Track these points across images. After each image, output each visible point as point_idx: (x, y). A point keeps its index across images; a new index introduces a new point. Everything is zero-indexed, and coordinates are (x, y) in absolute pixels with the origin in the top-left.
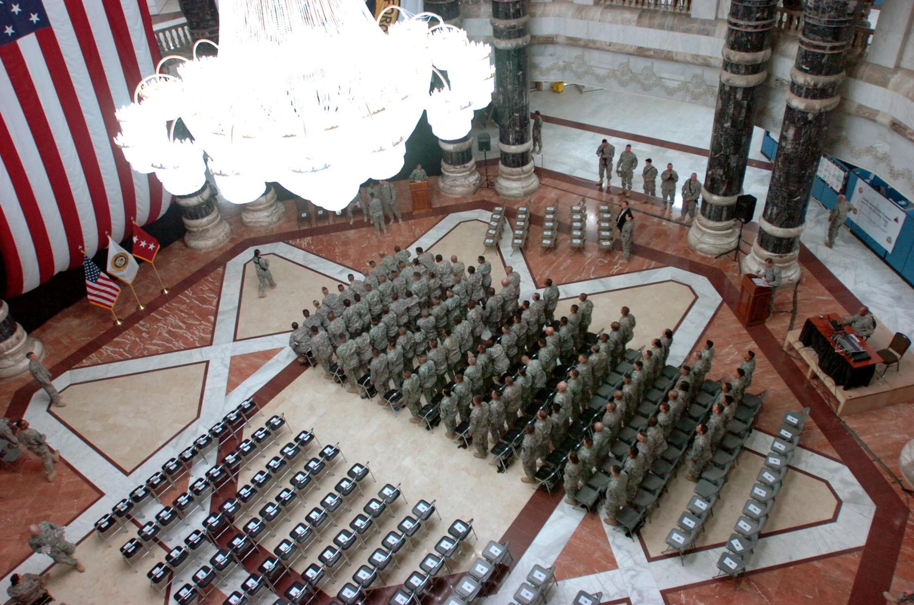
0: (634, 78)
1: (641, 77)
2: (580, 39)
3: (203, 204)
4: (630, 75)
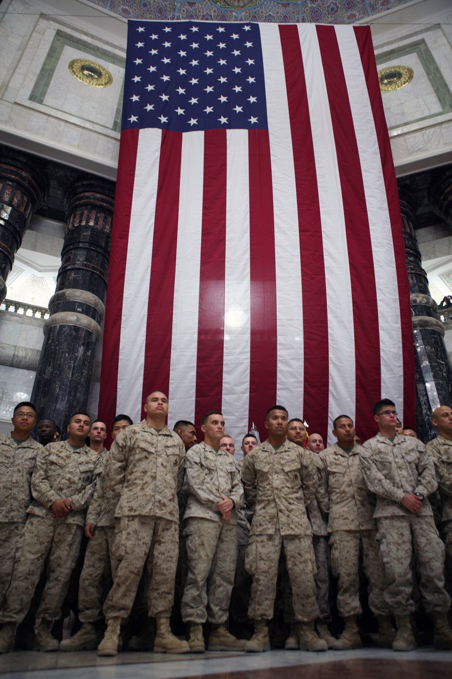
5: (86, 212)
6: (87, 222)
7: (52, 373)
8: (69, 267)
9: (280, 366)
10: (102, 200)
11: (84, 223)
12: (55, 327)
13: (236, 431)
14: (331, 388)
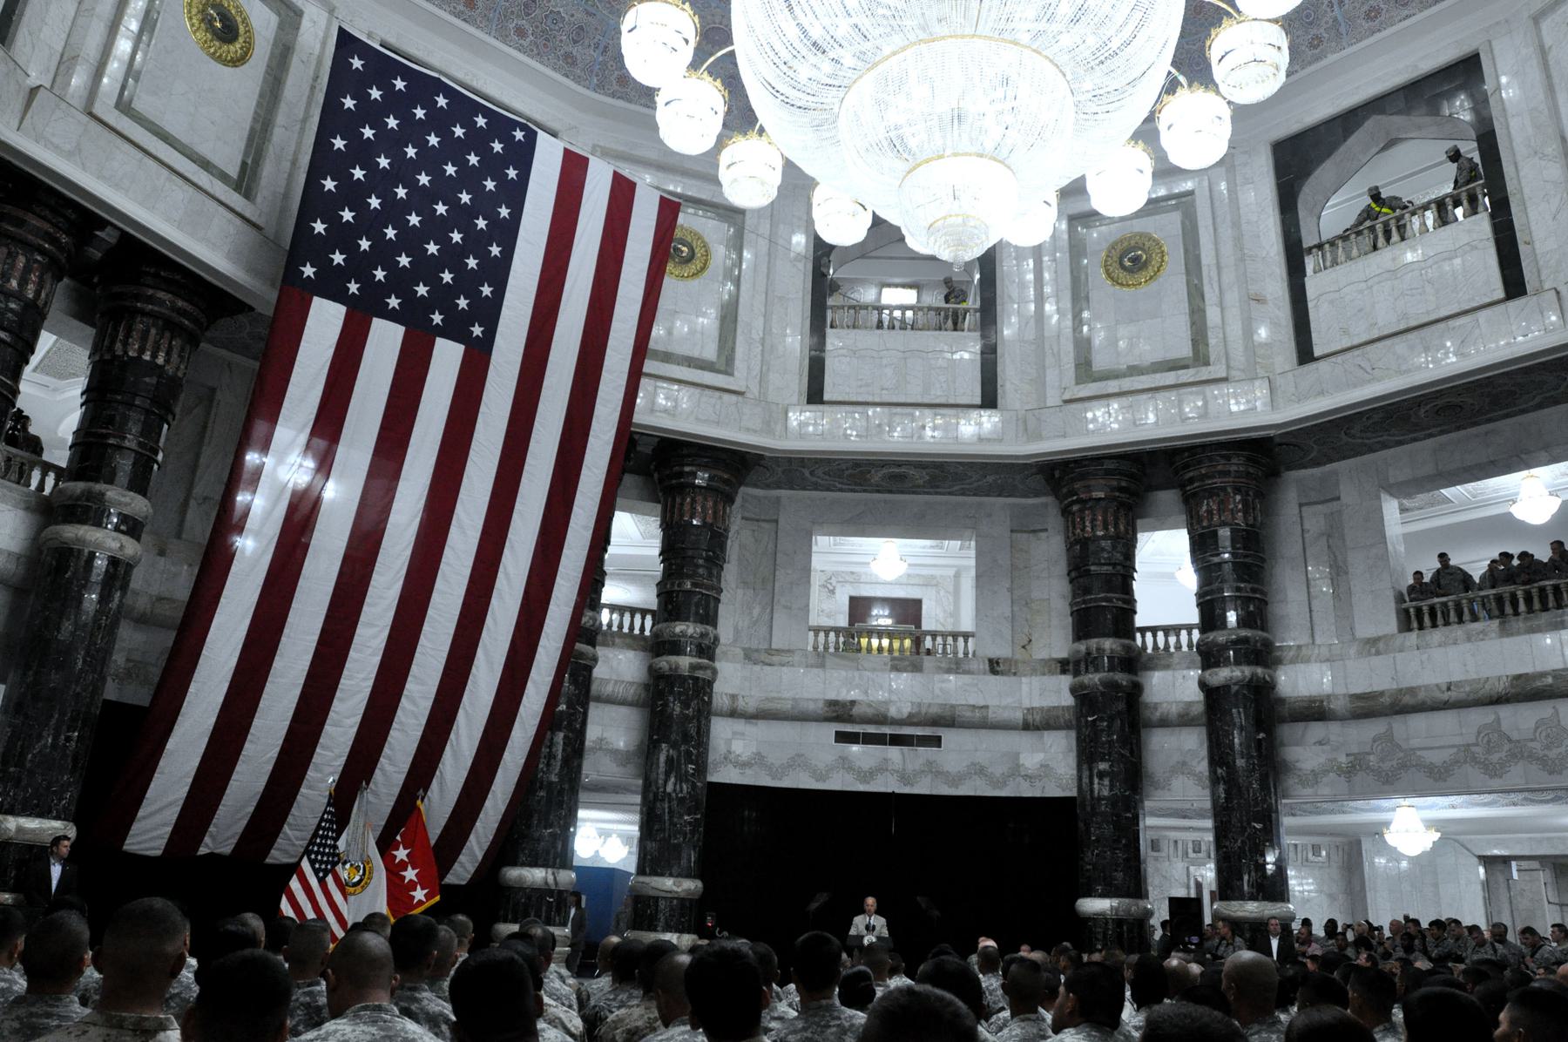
0: (1519, 752)
1: (1536, 746)
2: (1382, 693)
3: (550, 892)
4: (1506, 747)
5: (153, 331)
6: (154, 356)
7: (73, 634)
8: (111, 441)
9: (404, 701)
10: (182, 312)
11: (147, 357)
12: (80, 551)
13: (328, 770)
14: (452, 736)
